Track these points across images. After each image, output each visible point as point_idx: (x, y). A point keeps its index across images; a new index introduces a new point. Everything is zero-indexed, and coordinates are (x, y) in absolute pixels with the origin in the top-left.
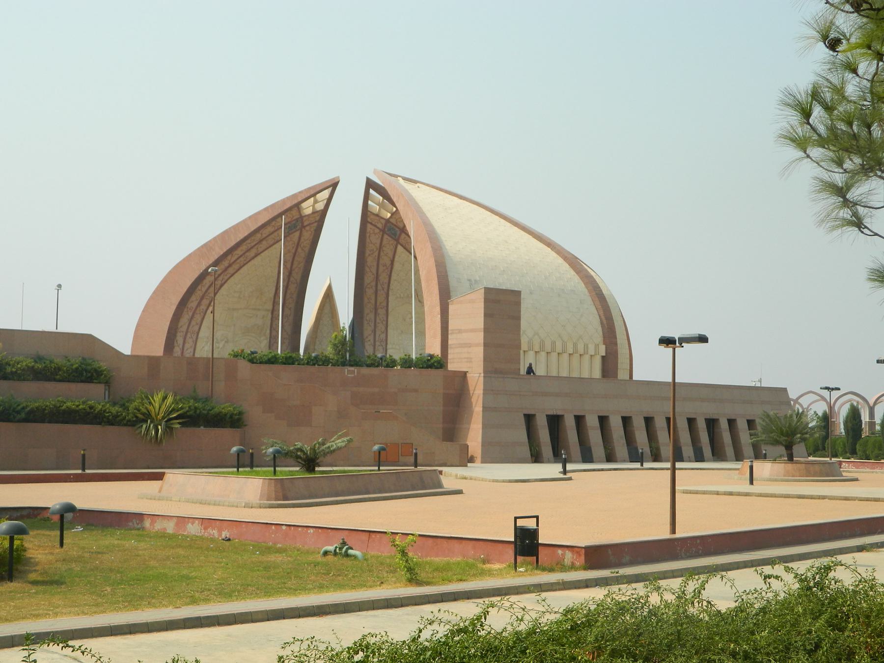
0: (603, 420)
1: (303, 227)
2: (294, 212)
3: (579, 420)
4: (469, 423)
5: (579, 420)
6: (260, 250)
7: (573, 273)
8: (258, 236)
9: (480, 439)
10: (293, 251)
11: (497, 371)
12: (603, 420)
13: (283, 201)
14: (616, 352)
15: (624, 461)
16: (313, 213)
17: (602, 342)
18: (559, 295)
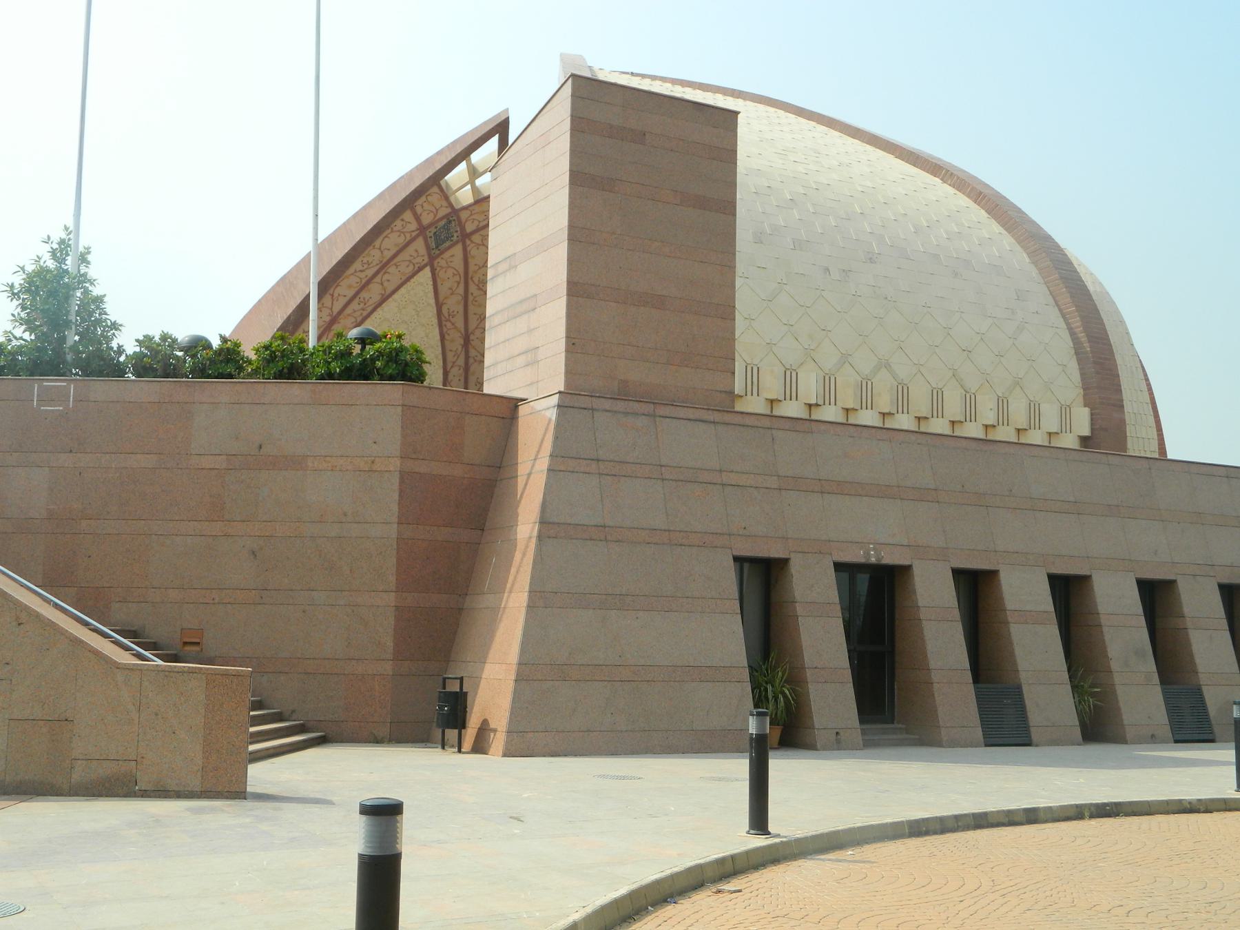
0: (1068, 592)
1: (465, 236)
2: (434, 196)
3: (975, 587)
4: (499, 589)
5: (975, 587)
6: (390, 288)
7: (996, 228)
8: (374, 255)
9: (513, 655)
10: (461, 290)
11: (624, 393)
12: (1068, 592)
13: (410, 175)
14: (1122, 424)
15: (1153, 739)
16: (477, 202)
17: (1081, 400)
18: (956, 274)
